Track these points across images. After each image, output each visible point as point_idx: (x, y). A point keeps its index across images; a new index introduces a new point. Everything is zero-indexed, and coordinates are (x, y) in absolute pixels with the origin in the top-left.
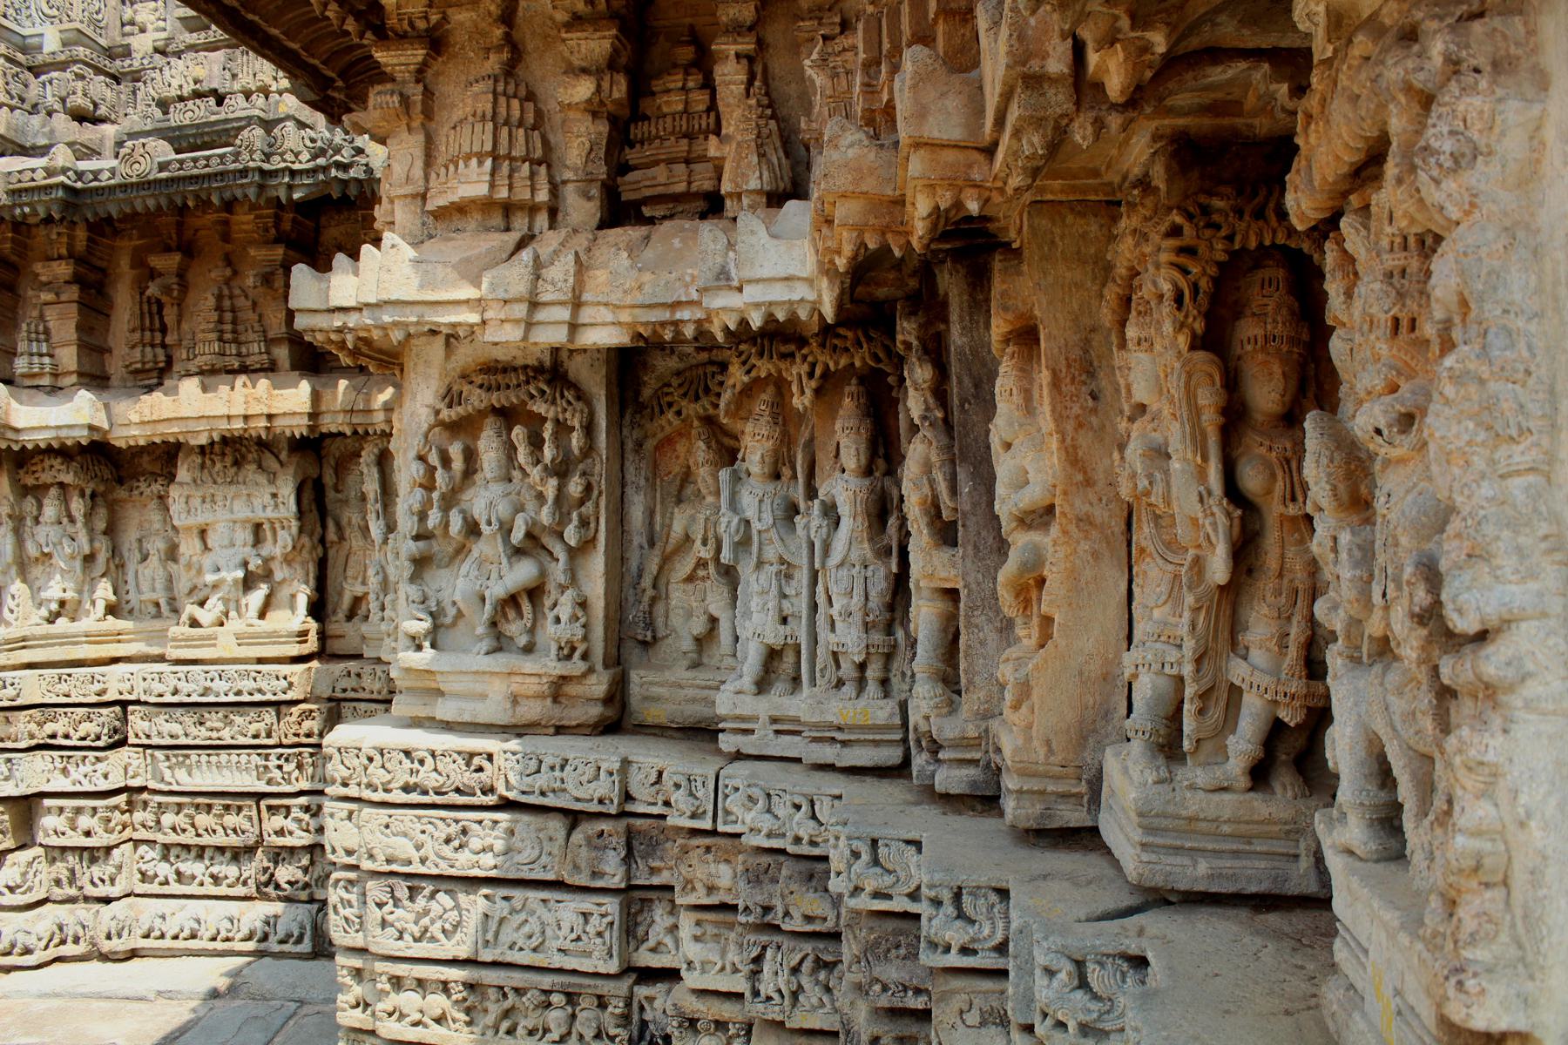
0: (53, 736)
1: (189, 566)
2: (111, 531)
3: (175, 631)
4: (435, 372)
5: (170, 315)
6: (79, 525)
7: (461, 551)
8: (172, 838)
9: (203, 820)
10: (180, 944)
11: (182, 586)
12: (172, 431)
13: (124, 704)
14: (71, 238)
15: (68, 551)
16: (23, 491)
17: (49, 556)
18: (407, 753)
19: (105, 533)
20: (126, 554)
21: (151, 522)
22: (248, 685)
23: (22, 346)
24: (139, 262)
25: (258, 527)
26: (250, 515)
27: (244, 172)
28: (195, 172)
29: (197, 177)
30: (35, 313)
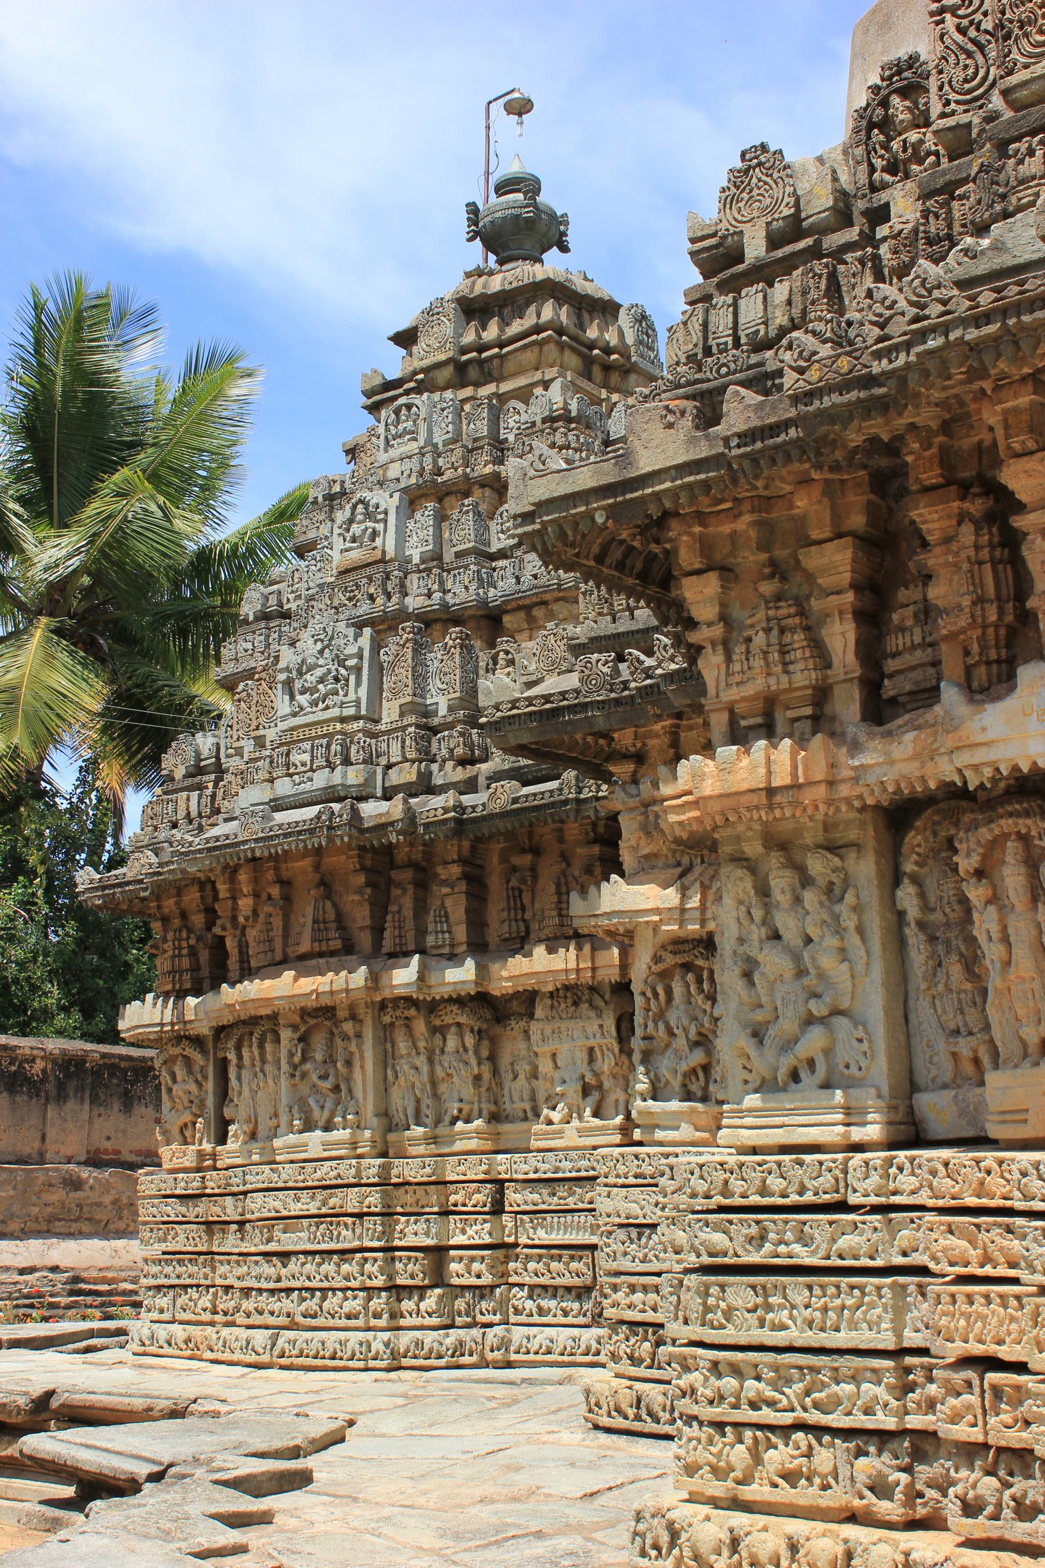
0: (455, 1205)
1: (545, 1079)
2: (492, 1058)
3: (536, 1128)
4: (650, 945)
5: (526, 899)
6: (471, 1053)
7: (668, 1045)
8: (536, 1280)
9: (554, 1265)
10: (539, 1358)
11: (541, 1096)
12: (531, 983)
13: (501, 1182)
14: (460, 846)
16: (434, 1030)
18: (637, 1157)
19: (488, 1059)
21: (520, 1050)
22: (585, 1163)
23: (431, 927)
24: (504, 858)
25: (591, 1050)
27: (566, 802)
28: (536, 803)
29: (537, 806)
30: (439, 903)
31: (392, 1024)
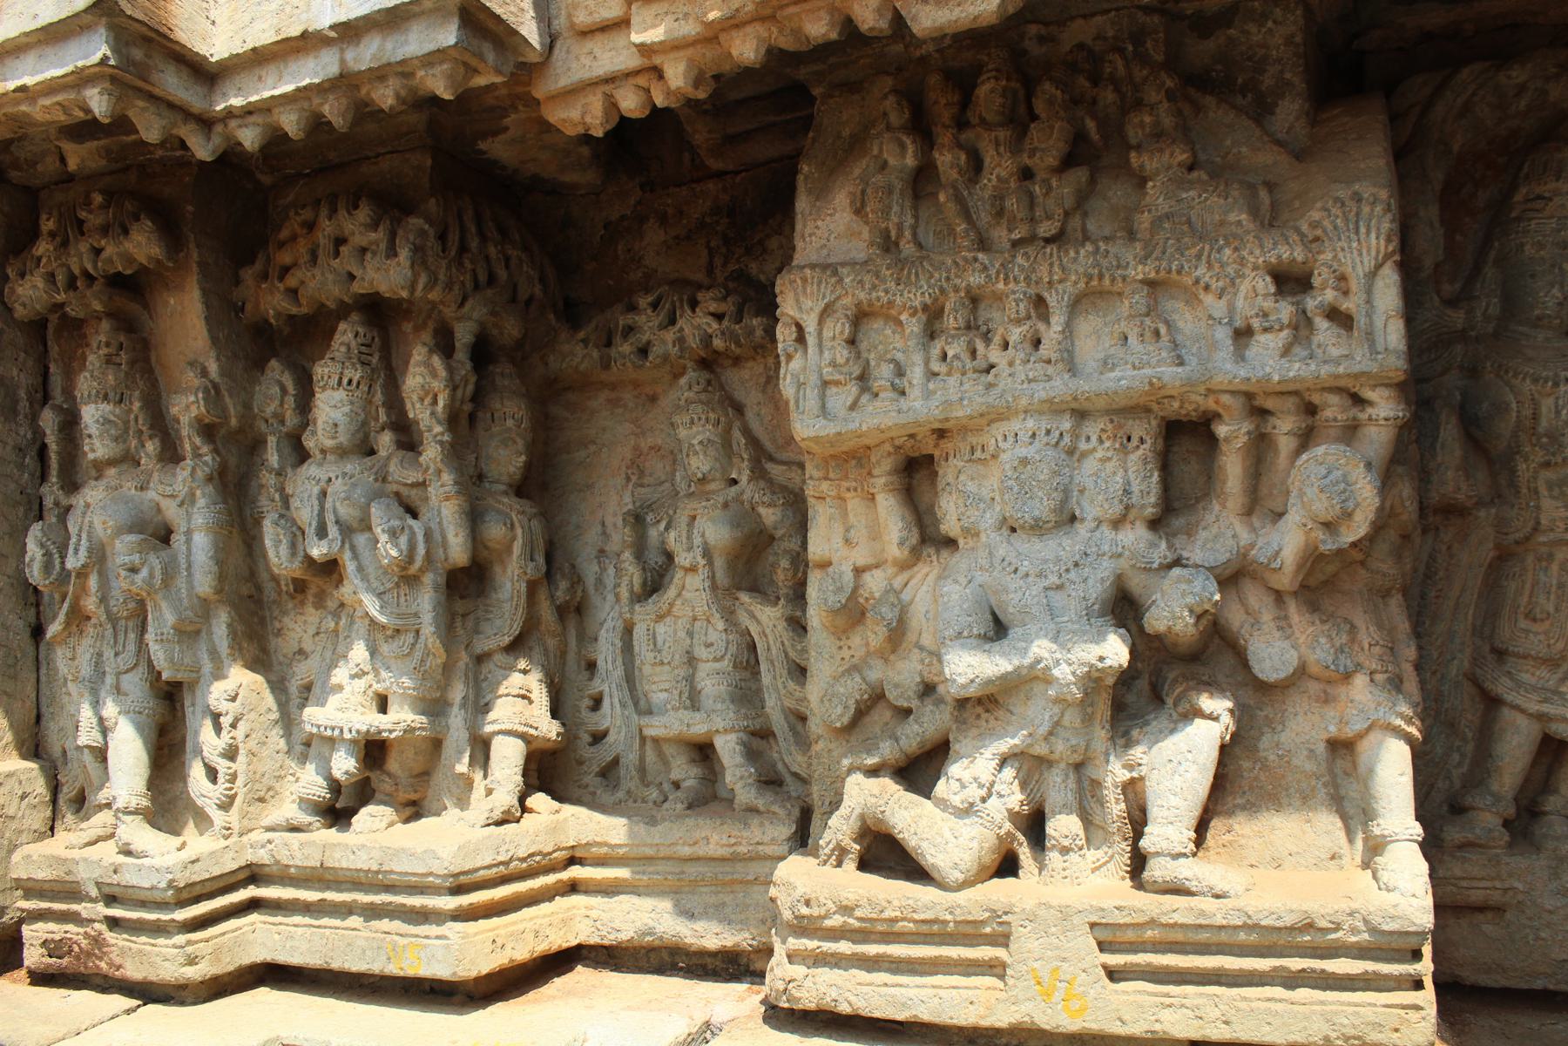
6: (431, 453)
15: (390, 551)
17: (330, 569)
20: (590, 570)
26: (1170, 374)
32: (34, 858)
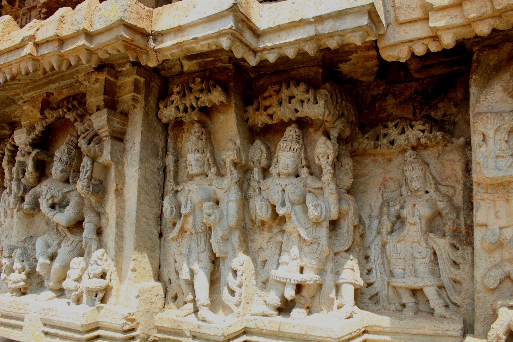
6: (327, 176)
31: (179, 124)
32: (164, 319)
